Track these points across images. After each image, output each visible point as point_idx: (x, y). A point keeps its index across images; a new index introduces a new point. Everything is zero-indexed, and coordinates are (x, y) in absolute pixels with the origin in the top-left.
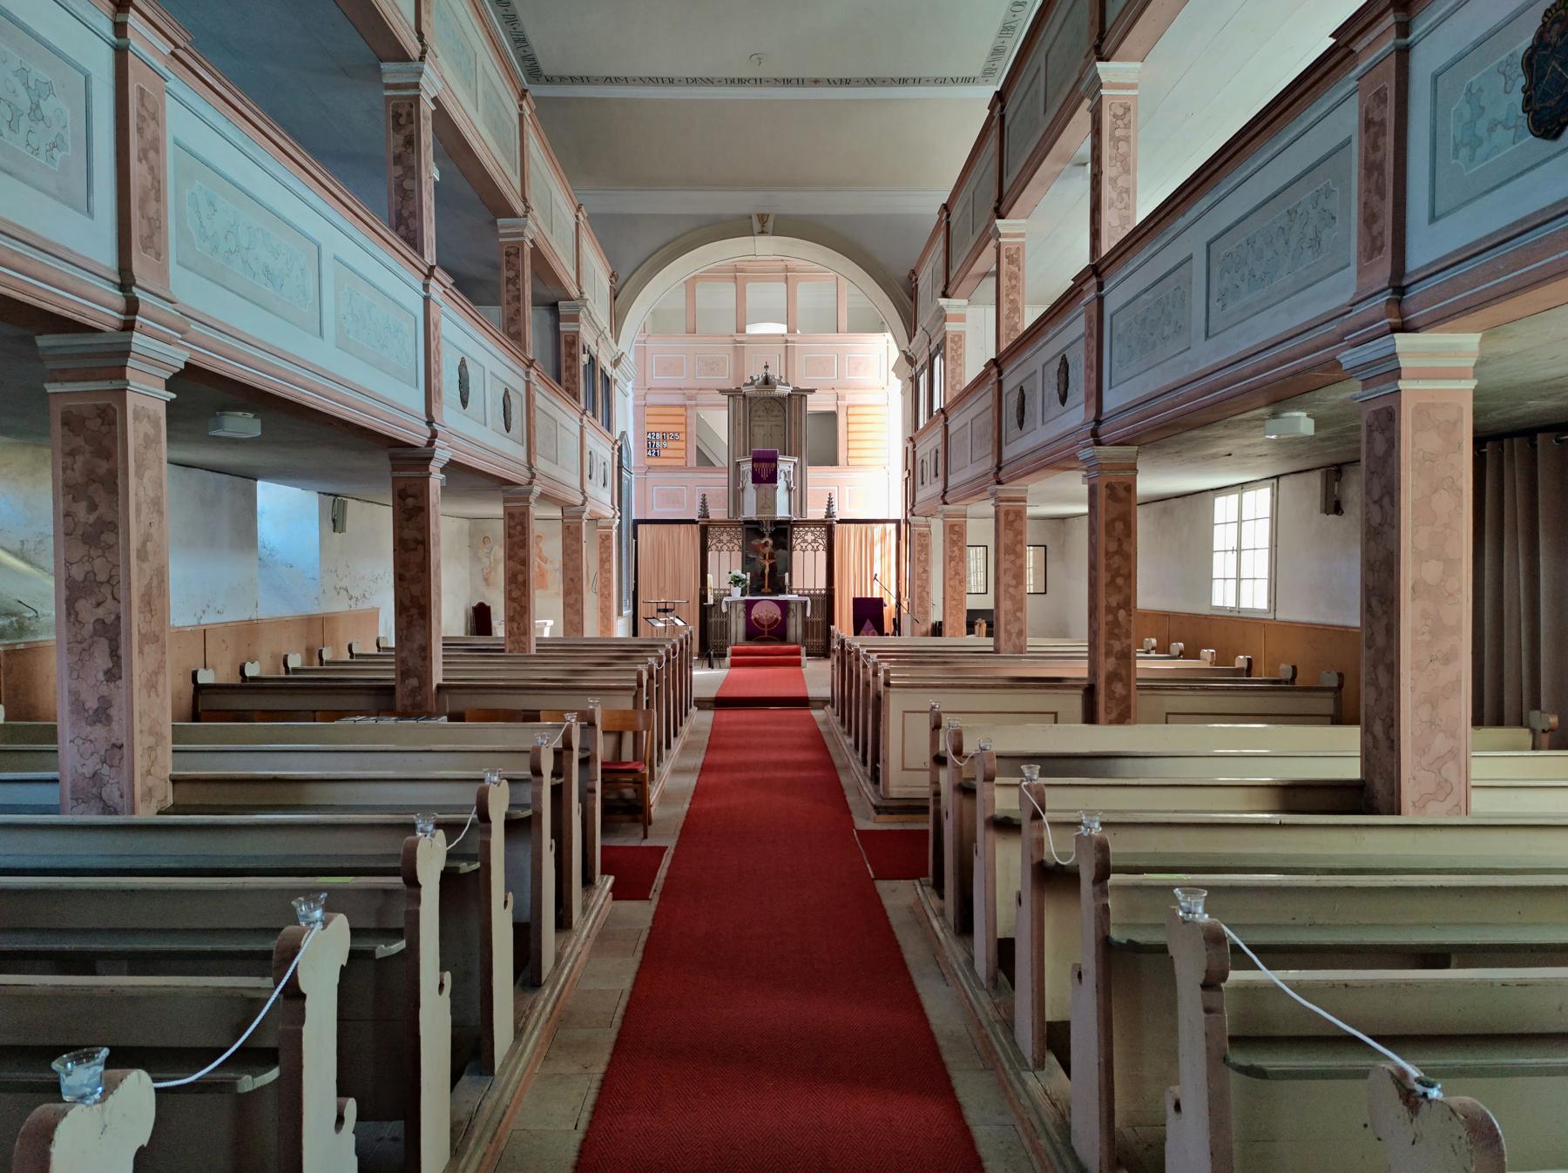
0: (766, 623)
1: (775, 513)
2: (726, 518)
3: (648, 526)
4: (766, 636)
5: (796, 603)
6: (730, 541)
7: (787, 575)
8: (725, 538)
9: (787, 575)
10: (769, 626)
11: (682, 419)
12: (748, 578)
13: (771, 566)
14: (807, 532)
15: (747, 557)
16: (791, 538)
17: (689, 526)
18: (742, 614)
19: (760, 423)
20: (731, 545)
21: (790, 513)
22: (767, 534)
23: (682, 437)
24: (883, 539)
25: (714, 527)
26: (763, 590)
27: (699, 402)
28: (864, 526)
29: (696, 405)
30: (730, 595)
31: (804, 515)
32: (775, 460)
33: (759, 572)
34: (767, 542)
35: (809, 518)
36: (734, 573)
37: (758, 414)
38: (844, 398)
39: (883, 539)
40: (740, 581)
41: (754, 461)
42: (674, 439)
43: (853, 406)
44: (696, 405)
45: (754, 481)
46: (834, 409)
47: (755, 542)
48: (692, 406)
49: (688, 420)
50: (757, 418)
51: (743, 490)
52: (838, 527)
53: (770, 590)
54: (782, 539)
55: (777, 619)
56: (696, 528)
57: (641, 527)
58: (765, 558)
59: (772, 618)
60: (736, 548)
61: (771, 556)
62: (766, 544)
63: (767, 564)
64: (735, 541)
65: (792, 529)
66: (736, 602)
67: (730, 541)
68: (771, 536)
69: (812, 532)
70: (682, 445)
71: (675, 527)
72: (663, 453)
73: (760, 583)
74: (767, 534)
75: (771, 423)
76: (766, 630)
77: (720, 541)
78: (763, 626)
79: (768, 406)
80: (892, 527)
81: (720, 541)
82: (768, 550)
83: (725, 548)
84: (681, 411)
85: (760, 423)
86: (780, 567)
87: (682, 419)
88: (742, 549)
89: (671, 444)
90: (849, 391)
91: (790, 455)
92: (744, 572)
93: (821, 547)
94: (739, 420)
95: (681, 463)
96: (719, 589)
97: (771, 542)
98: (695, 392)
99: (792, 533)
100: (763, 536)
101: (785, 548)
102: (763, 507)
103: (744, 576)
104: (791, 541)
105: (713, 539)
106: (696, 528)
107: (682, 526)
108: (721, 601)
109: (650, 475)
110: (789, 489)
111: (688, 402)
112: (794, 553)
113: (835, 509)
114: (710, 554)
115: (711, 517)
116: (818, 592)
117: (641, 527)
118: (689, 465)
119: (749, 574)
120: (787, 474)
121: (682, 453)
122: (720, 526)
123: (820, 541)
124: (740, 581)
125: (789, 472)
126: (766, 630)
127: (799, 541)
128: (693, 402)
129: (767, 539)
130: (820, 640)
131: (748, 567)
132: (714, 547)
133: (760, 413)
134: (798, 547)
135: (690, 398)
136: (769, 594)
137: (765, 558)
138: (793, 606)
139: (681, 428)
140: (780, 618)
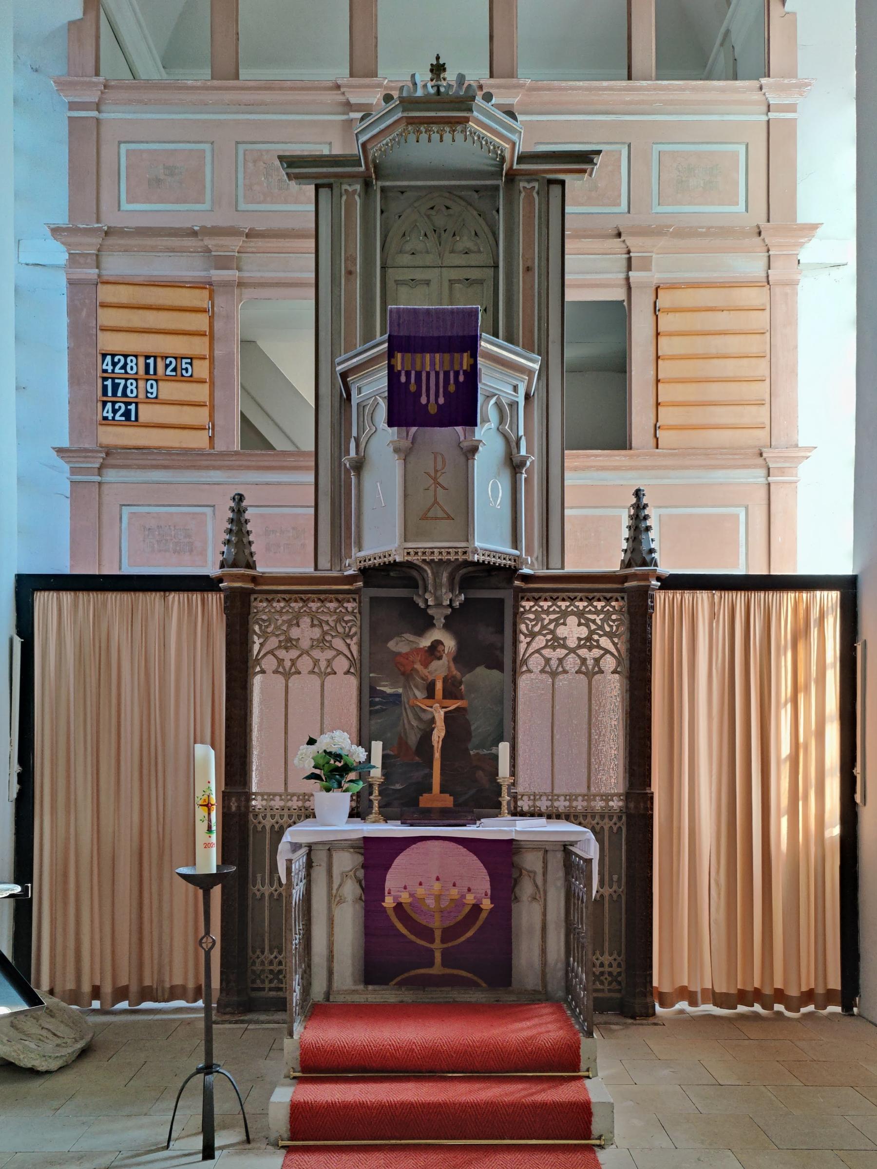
0: (436, 924)
1: (467, 531)
2: (308, 569)
3: (67, 597)
4: (437, 969)
5: (543, 848)
6: (322, 643)
7: (504, 749)
8: (305, 632)
9: (504, 749)
10: (449, 933)
11: (200, 322)
12: (377, 759)
13: (449, 718)
14: (565, 614)
15: (373, 691)
16: (515, 632)
17: (196, 597)
18: (351, 890)
19: (419, 275)
20: (323, 656)
21: (515, 544)
22: (439, 616)
23: (201, 369)
24: (800, 634)
25: (270, 596)
26: (425, 801)
27: (246, 274)
28: (739, 598)
29: (241, 284)
30: (310, 814)
31: (555, 560)
32: (470, 345)
33: (413, 739)
34: (437, 644)
35: (571, 567)
36: (325, 742)
37: (408, 247)
38: (646, 265)
39: (800, 634)
40: (346, 769)
41: (396, 345)
42: (179, 376)
43: (673, 286)
44: (241, 284)
45: (390, 424)
46: (619, 295)
47: (399, 645)
48: (226, 285)
49: (217, 325)
50: (406, 259)
51: (359, 466)
52: (662, 599)
53: (448, 801)
54: (485, 634)
55: (476, 908)
56: (214, 600)
57: (43, 601)
58: (430, 693)
59: (459, 903)
60: (342, 664)
61: (452, 690)
62: (434, 650)
63: (440, 715)
64: (338, 643)
65: (516, 606)
66: (331, 847)
67: (322, 643)
68: (449, 625)
69: (580, 614)
70: (201, 393)
71: (154, 599)
72: (147, 413)
73: (417, 775)
74: (439, 616)
75: (455, 274)
76: (437, 946)
77: (289, 643)
78: (427, 933)
79: (440, 220)
80: (832, 597)
81: (289, 643)
82: (439, 669)
83: (305, 664)
84: (200, 298)
85: (419, 275)
86: (479, 726)
87: (200, 322)
88: (357, 667)
89: (168, 390)
90: (663, 242)
91: (511, 339)
92: (363, 741)
93: (609, 663)
94: (350, 259)
95: (199, 440)
96: (287, 795)
97: (450, 644)
98: (237, 243)
99: (517, 615)
100: (425, 623)
101: (500, 667)
102: (424, 518)
103: (360, 754)
104: (515, 642)
105: (265, 635)
106: (214, 600)
107: (175, 598)
108: (278, 834)
109: (111, 475)
110: (514, 465)
111: (217, 275)
112: (523, 682)
113: (655, 538)
114: (257, 682)
115: (261, 569)
116: (599, 805)
117: (43, 601)
118: (220, 446)
119: (377, 747)
120: (505, 411)
121: (201, 416)
122: (289, 596)
123: (605, 642)
124: (346, 769)
125: (513, 405)
126: (437, 946)
127: (540, 642)
128: (231, 275)
129: (437, 634)
130: (607, 959)
131: (376, 723)
132: (269, 663)
133: (415, 242)
134: (535, 662)
135: (223, 263)
136: (445, 816)
137: (430, 693)
138: (531, 861)
139: (199, 346)
140: (487, 904)
